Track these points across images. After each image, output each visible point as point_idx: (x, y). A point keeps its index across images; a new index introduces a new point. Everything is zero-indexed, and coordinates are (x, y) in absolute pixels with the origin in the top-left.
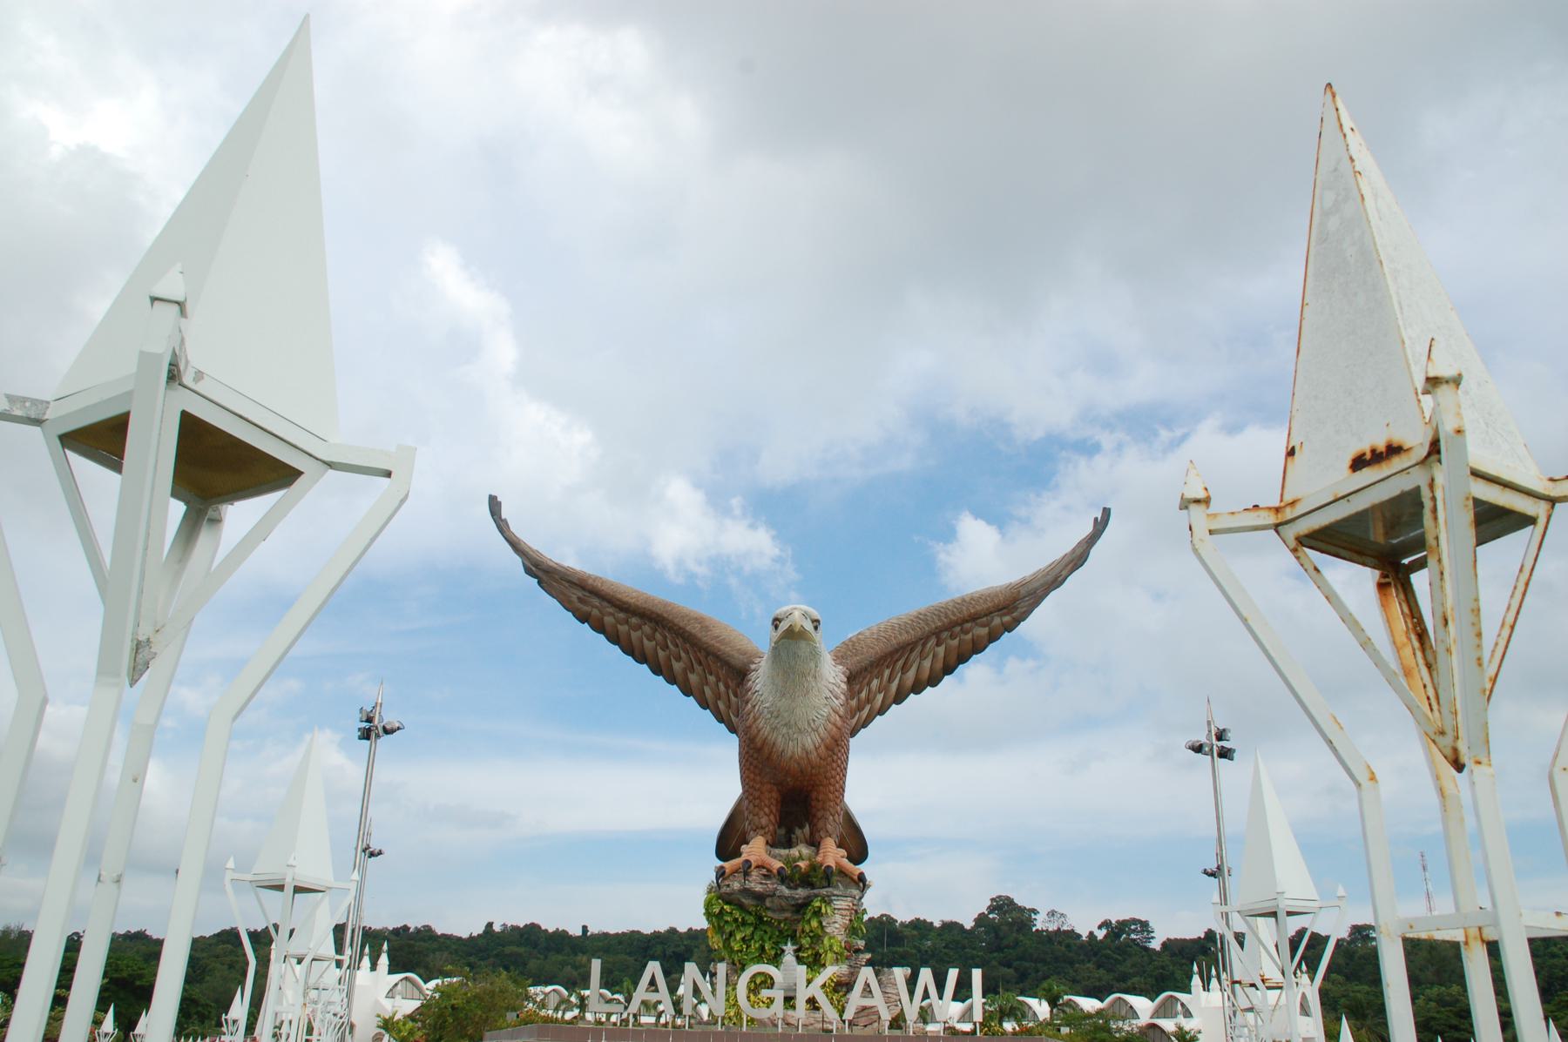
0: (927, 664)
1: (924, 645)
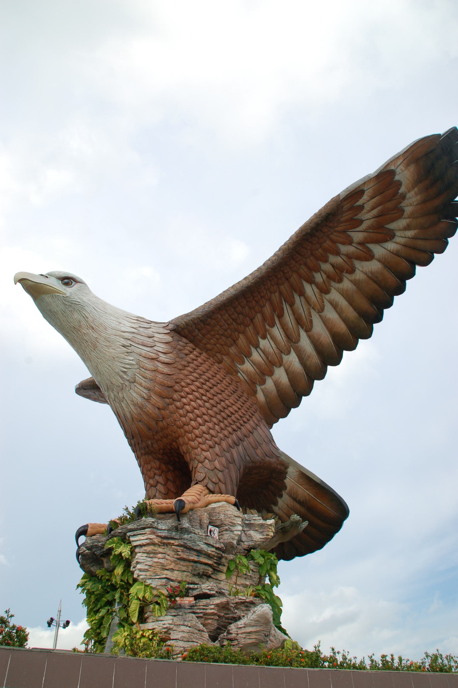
0: (331, 314)
1: (302, 293)
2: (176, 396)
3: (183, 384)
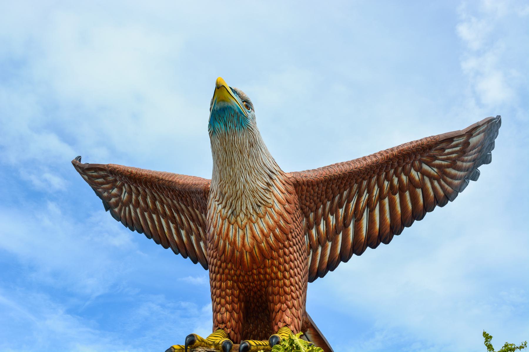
3: (293, 234)
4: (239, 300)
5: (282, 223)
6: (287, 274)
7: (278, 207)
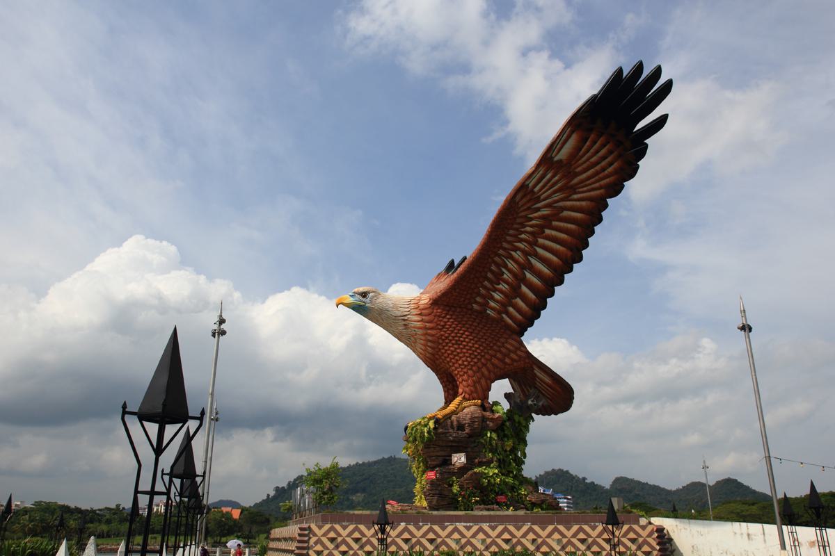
2: (440, 347)
3: (443, 338)
4: (450, 382)
5: (430, 338)
6: (451, 364)
7: (420, 332)
